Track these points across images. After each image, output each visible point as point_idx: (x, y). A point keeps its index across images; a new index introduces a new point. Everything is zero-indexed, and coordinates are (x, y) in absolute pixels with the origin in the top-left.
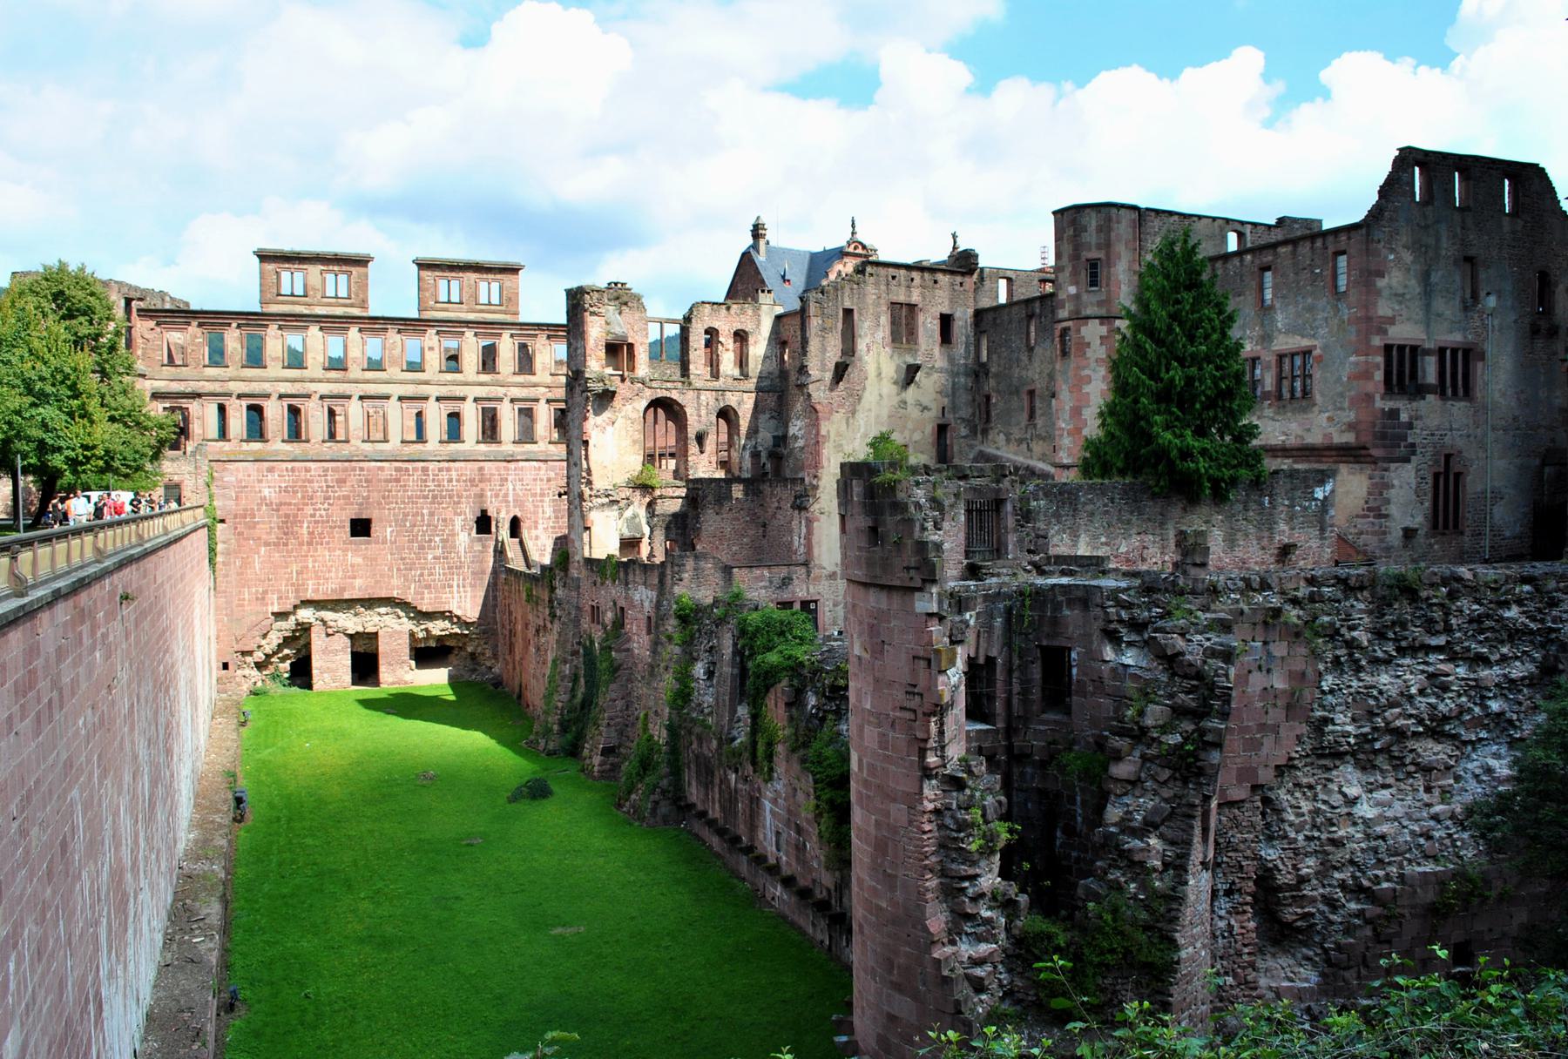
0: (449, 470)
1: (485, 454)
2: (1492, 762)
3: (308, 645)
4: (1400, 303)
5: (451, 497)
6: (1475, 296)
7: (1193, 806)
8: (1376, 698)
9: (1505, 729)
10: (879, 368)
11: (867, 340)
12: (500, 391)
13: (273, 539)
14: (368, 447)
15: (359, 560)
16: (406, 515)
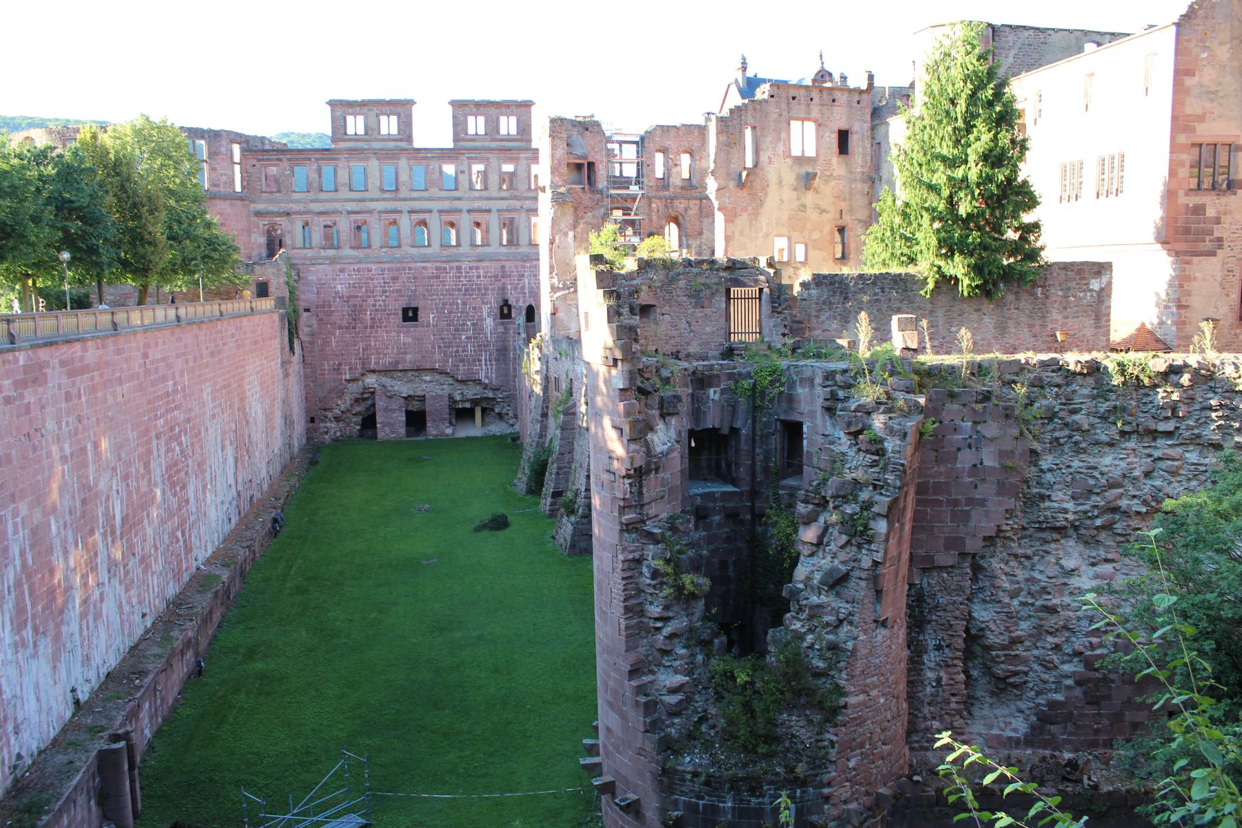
3: (374, 405)
5: (479, 290)
10: (780, 176)
11: (769, 153)
12: (518, 204)
13: (344, 323)
14: (414, 251)
15: (410, 340)
16: (444, 304)
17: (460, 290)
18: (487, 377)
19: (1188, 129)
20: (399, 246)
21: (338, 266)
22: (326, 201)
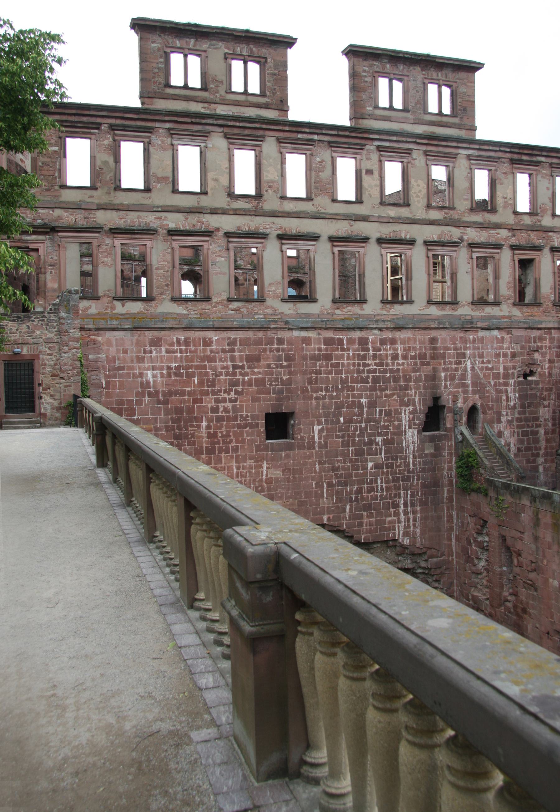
0: (393, 342)
1: (439, 320)
5: (396, 380)
12: (455, 233)
14: (287, 309)
16: (339, 406)
17: (364, 381)
18: (406, 534)
20: (261, 300)
21: (150, 335)
22: (128, 209)
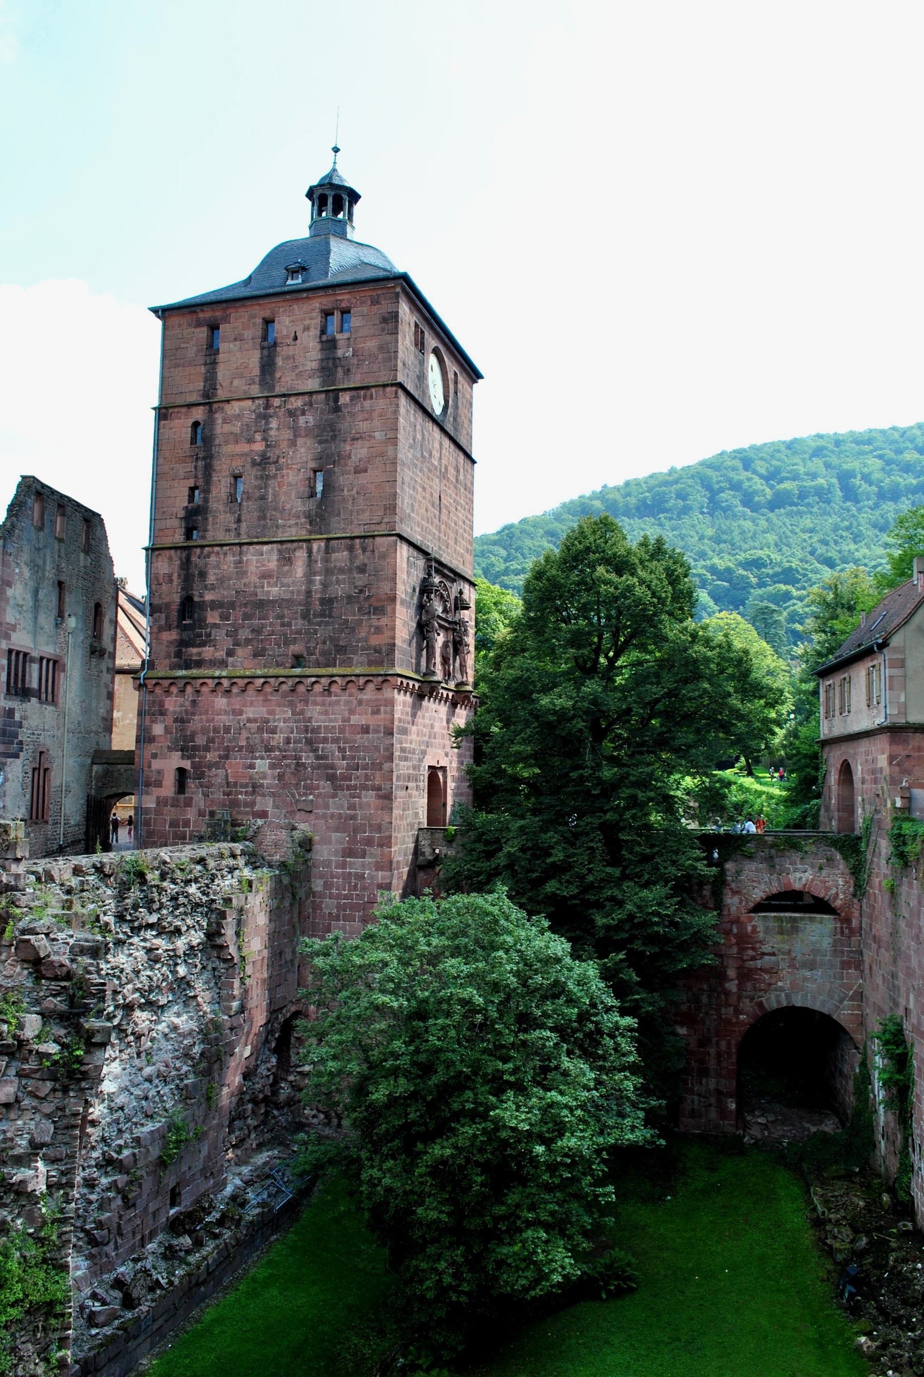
2: (177, 1021)
4: (20, 613)
6: (61, 614)
7: (76, 1115)
8: (119, 978)
9: (185, 990)
19: (7, 637)
